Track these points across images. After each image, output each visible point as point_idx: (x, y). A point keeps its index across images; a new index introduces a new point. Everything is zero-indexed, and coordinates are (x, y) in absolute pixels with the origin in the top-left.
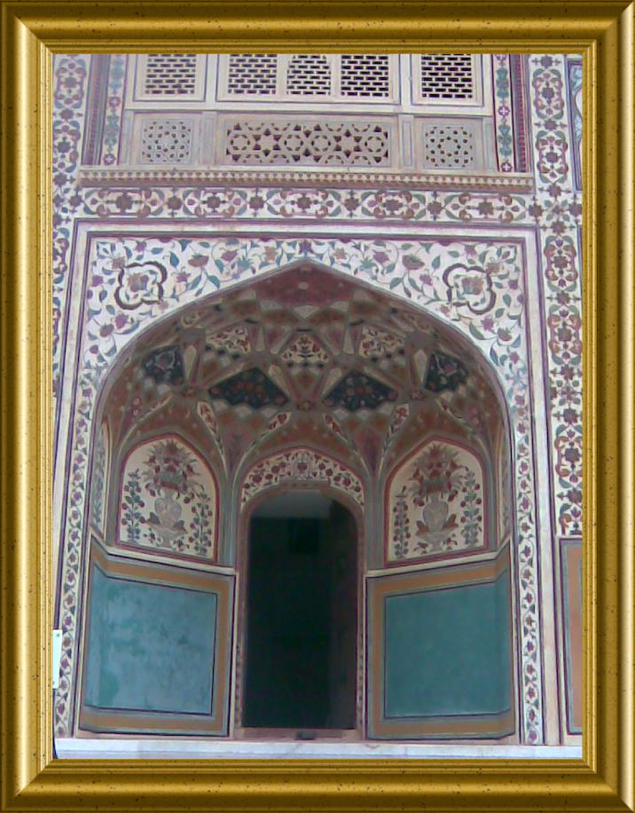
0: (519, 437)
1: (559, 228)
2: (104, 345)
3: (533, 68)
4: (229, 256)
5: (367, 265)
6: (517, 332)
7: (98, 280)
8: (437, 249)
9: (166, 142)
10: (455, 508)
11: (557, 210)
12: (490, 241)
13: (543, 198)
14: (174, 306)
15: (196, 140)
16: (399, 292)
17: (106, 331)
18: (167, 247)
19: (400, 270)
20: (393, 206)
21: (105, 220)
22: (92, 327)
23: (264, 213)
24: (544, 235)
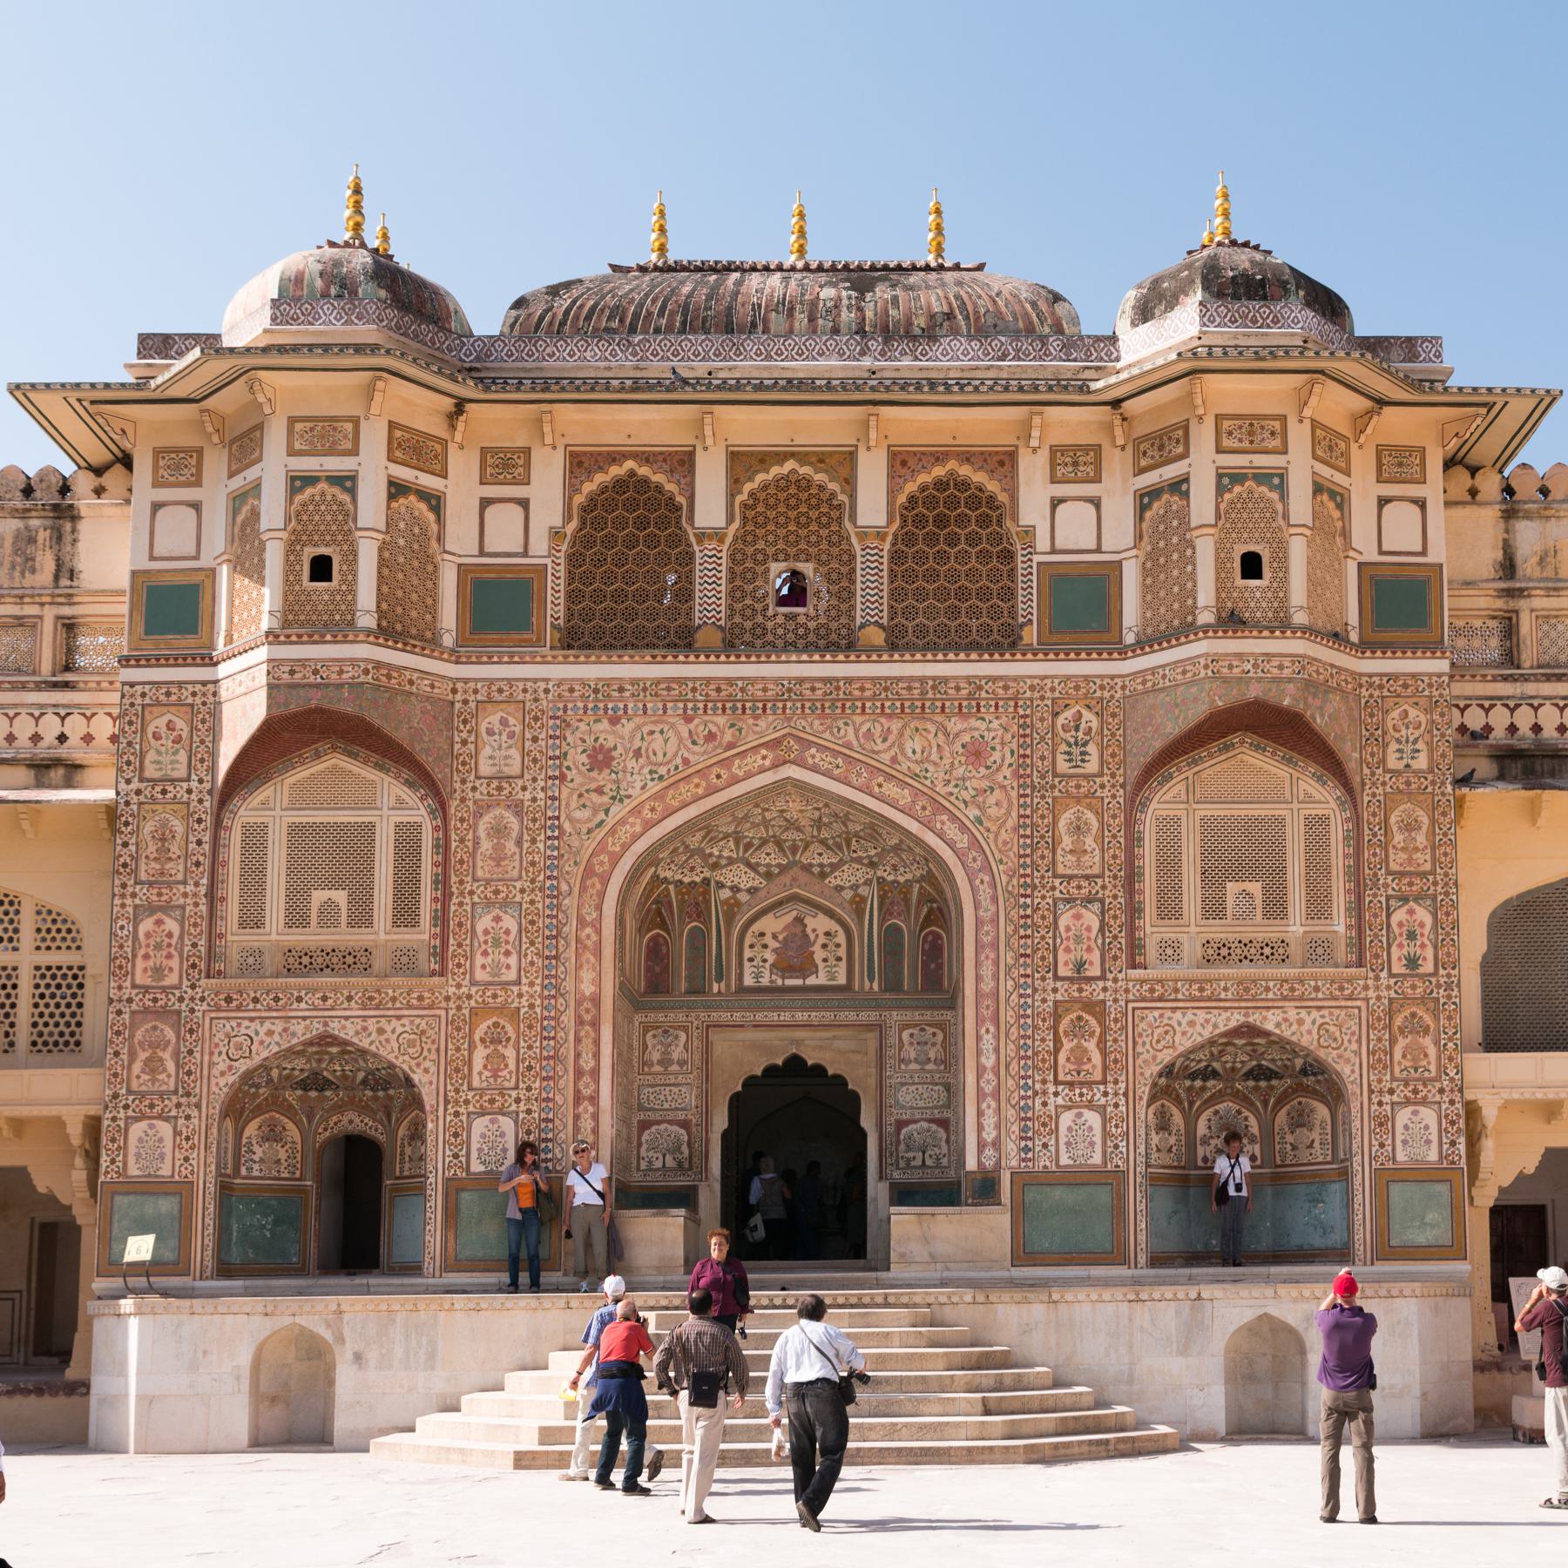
0: (430, 1126)
1: (459, 1008)
2: (222, 1082)
3: (453, 908)
4: (285, 1030)
5: (357, 1033)
6: (433, 1069)
7: (217, 1045)
8: (394, 1021)
9: (251, 960)
11: (459, 998)
12: (422, 1017)
13: (452, 990)
14: (257, 1060)
15: (267, 959)
16: (373, 1048)
17: (222, 1074)
18: (253, 1025)
19: (374, 1034)
20: (371, 998)
21: (218, 1010)
22: (215, 1072)
24: (451, 1013)
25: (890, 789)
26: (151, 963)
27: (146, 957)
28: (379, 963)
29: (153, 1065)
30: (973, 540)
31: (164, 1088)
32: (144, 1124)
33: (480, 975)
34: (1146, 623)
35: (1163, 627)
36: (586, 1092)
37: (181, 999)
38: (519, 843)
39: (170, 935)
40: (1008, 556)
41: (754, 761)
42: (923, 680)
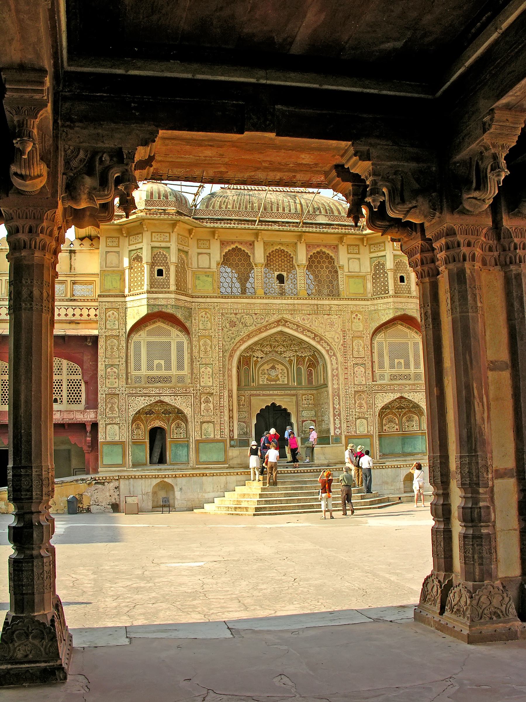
1: (197, 393)
9: (138, 380)
10: (181, 431)
15: (142, 379)
16: (173, 404)
23: (154, 392)
25: (309, 334)
26: (110, 380)
27: (109, 379)
28: (174, 380)
29: (112, 409)
30: (327, 268)
31: (115, 415)
32: (110, 426)
33: (202, 383)
34: (374, 292)
35: (379, 293)
36: (231, 416)
37: (119, 391)
38: (211, 347)
39: (115, 372)
40: (336, 272)
41: (273, 325)
42: (317, 305)
